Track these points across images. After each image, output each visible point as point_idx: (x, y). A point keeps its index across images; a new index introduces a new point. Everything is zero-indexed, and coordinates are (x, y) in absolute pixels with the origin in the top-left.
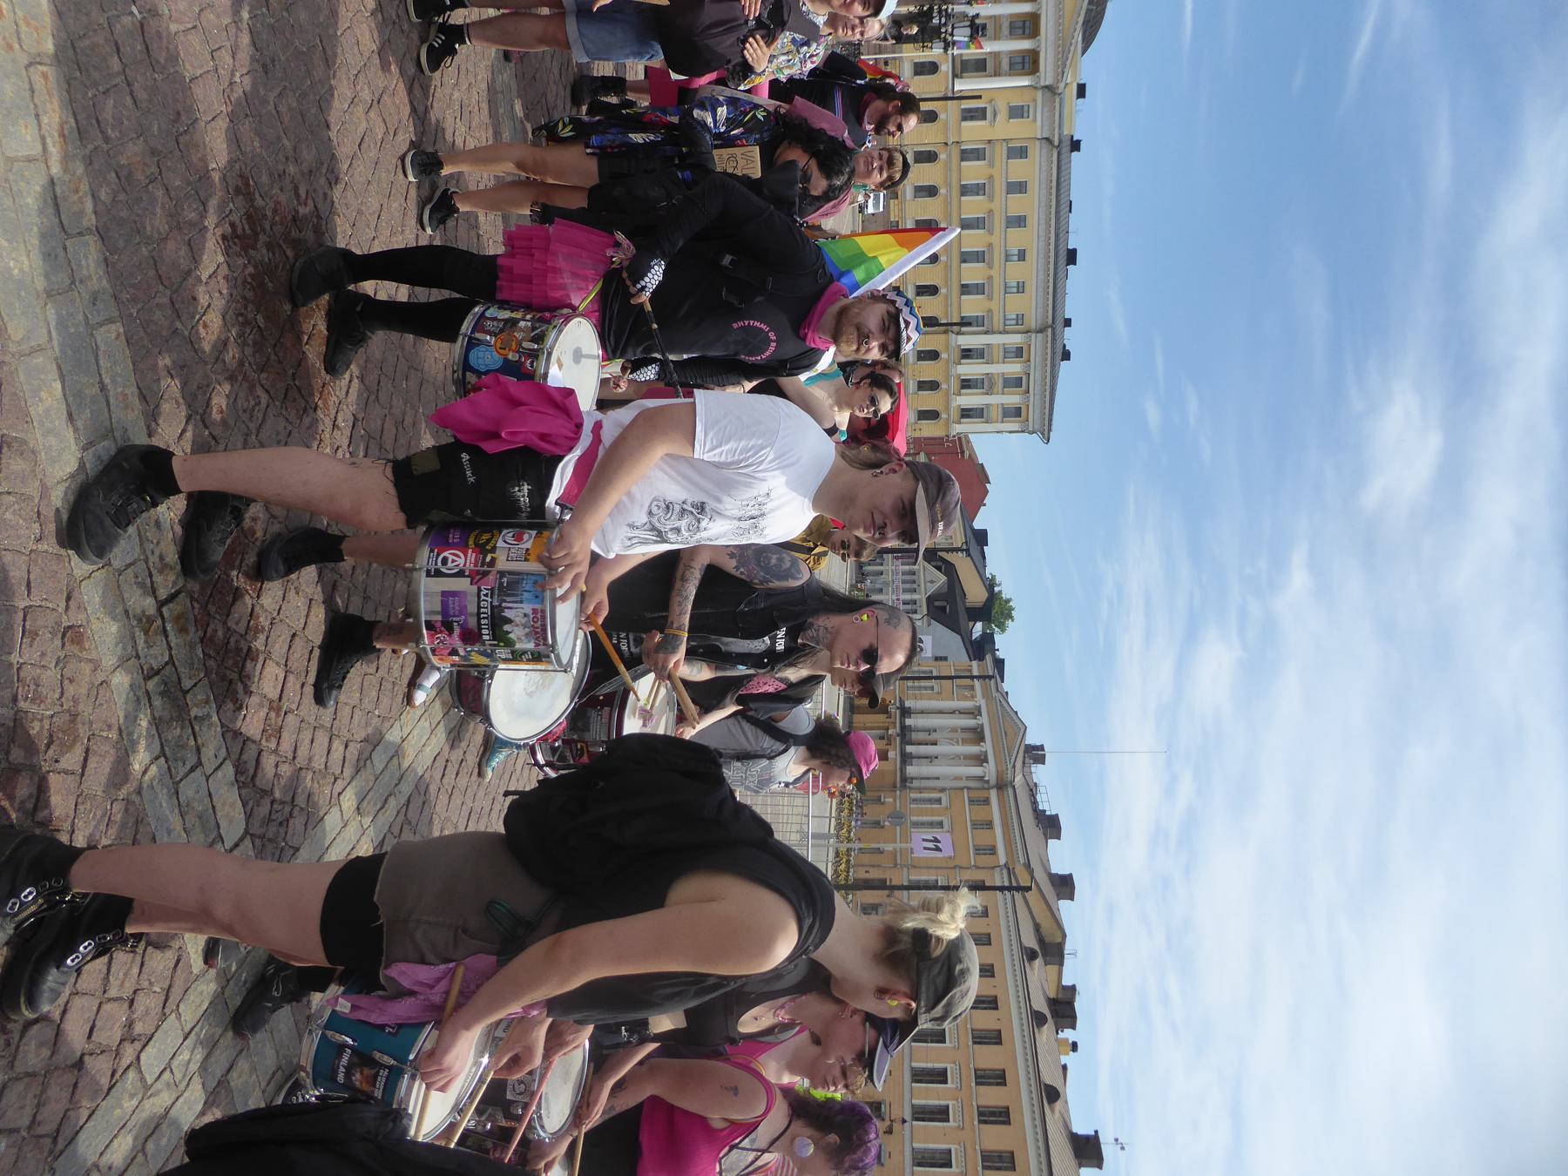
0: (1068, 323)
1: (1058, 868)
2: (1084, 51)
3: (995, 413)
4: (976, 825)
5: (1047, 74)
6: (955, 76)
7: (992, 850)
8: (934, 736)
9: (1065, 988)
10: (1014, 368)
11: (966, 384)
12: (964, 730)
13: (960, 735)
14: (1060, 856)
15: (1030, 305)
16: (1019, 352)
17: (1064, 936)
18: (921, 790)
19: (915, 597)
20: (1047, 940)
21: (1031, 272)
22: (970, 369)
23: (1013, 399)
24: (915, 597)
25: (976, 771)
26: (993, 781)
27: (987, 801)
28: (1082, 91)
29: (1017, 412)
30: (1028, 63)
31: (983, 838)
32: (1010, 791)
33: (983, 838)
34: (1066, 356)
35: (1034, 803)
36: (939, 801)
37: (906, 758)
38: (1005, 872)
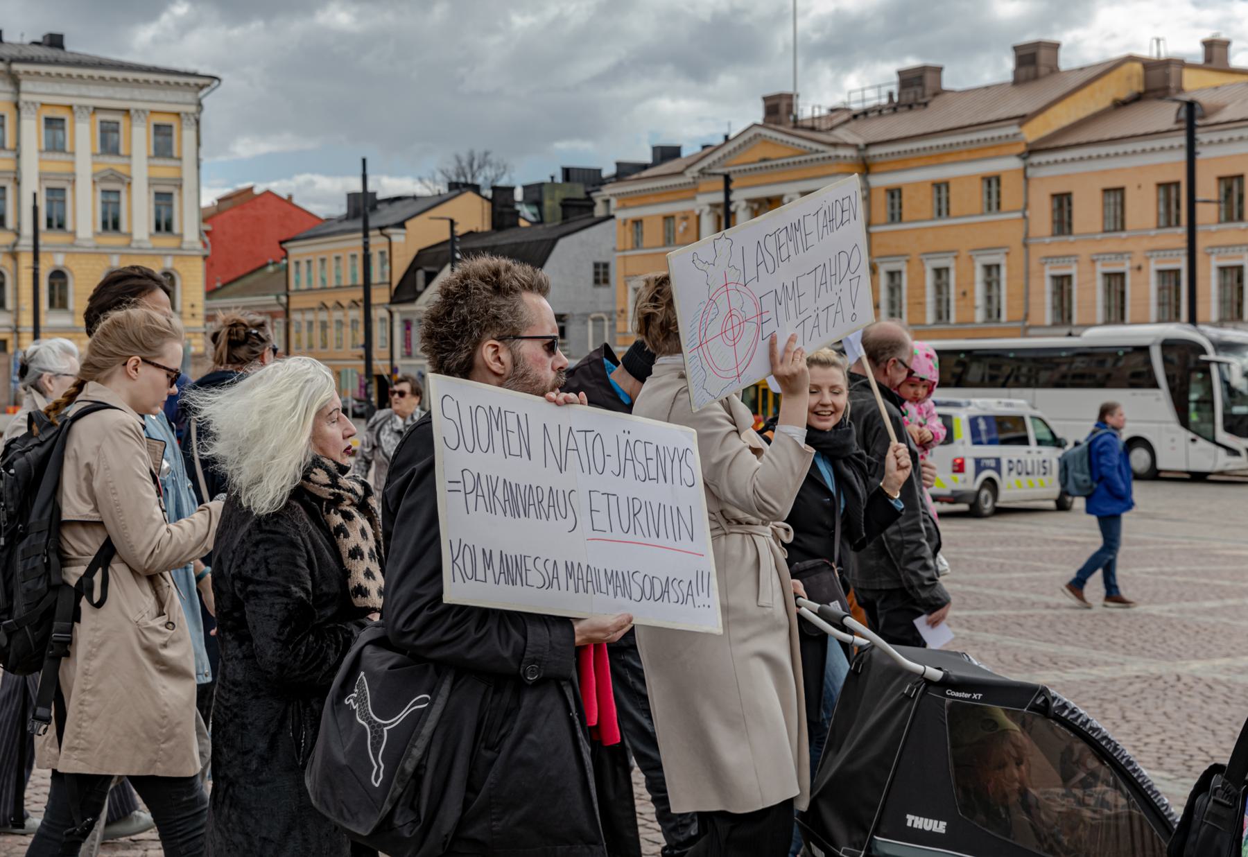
3: (165, 169)
4: (942, 208)
7: (993, 182)
10: (83, 134)
11: (111, 223)
17: (1131, 59)
23: (139, 138)
27: (894, 193)
29: (163, 132)
31: (967, 198)
32: (873, 151)
33: (967, 198)
34: (55, 41)
35: (879, 111)
36: (892, 275)
38: (1035, 159)
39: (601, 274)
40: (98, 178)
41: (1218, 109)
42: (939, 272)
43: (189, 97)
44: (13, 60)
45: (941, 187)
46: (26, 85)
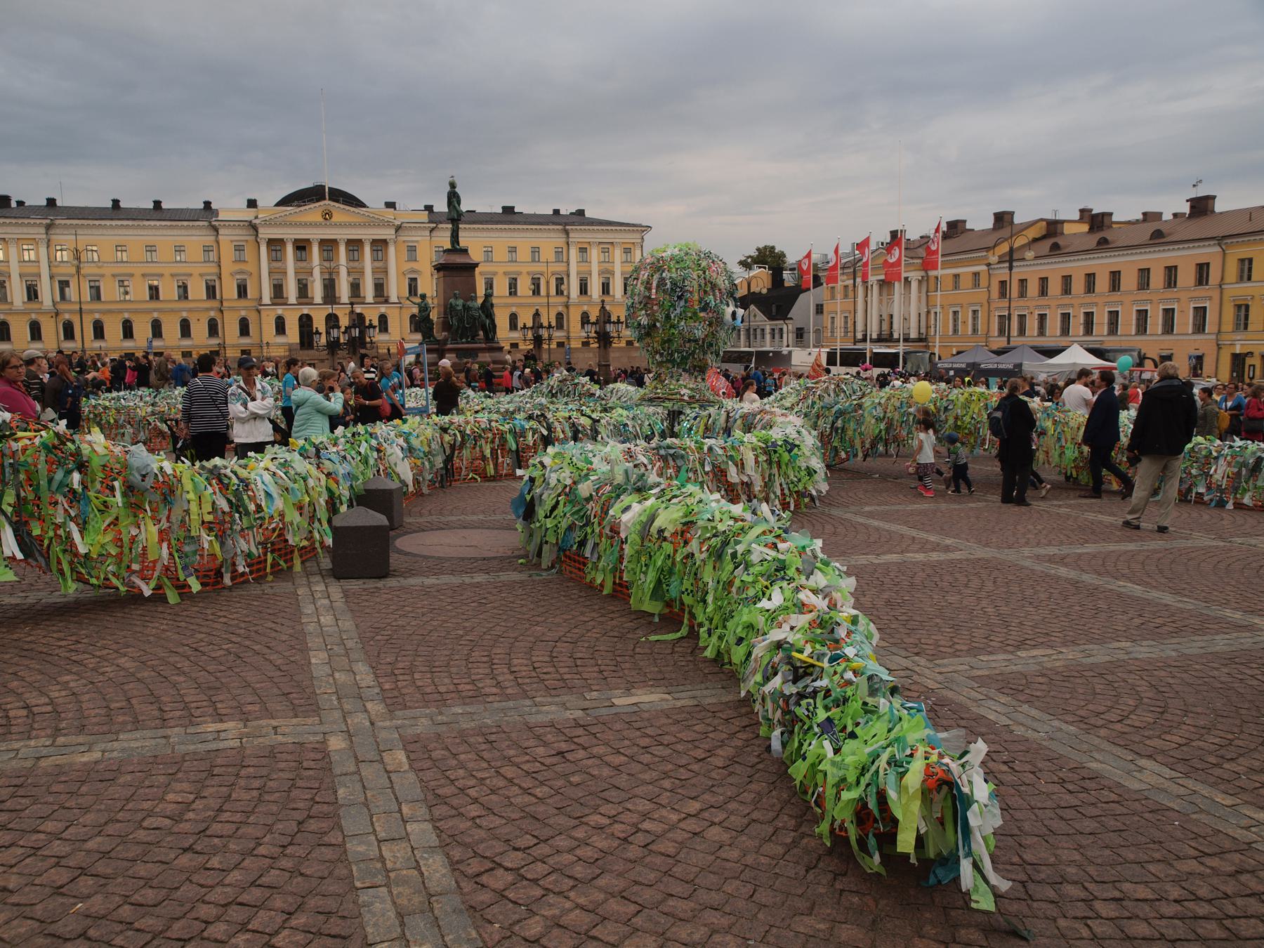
0: (556, 212)
1: (989, 224)
2: (362, 205)
4: (956, 287)
5: (387, 233)
6: (386, 301)
7: (976, 274)
8: (885, 317)
9: (1081, 218)
10: (594, 254)
12: (880, 294)
13: (885, 297)
14: (980, 221)
15: (549, 241)
16: (583, 250)
17: (1042, 220)
18: (928, 327)
19: (768, 330)
20: (1044, 233)
21: (524, 240)
24: (768, 330)
25: (914, 285)
26: (923, 273)
28: (390, 205)
30: (380, 245)
31: (966, 282)
33: (966, 282)
39: (819, 309)
40: (601, 273)
41: (1067, 247)
42: (955, 313)
43: (638, 236)
44: (566, 224)
45: (956, 276)
46: (571, 235)
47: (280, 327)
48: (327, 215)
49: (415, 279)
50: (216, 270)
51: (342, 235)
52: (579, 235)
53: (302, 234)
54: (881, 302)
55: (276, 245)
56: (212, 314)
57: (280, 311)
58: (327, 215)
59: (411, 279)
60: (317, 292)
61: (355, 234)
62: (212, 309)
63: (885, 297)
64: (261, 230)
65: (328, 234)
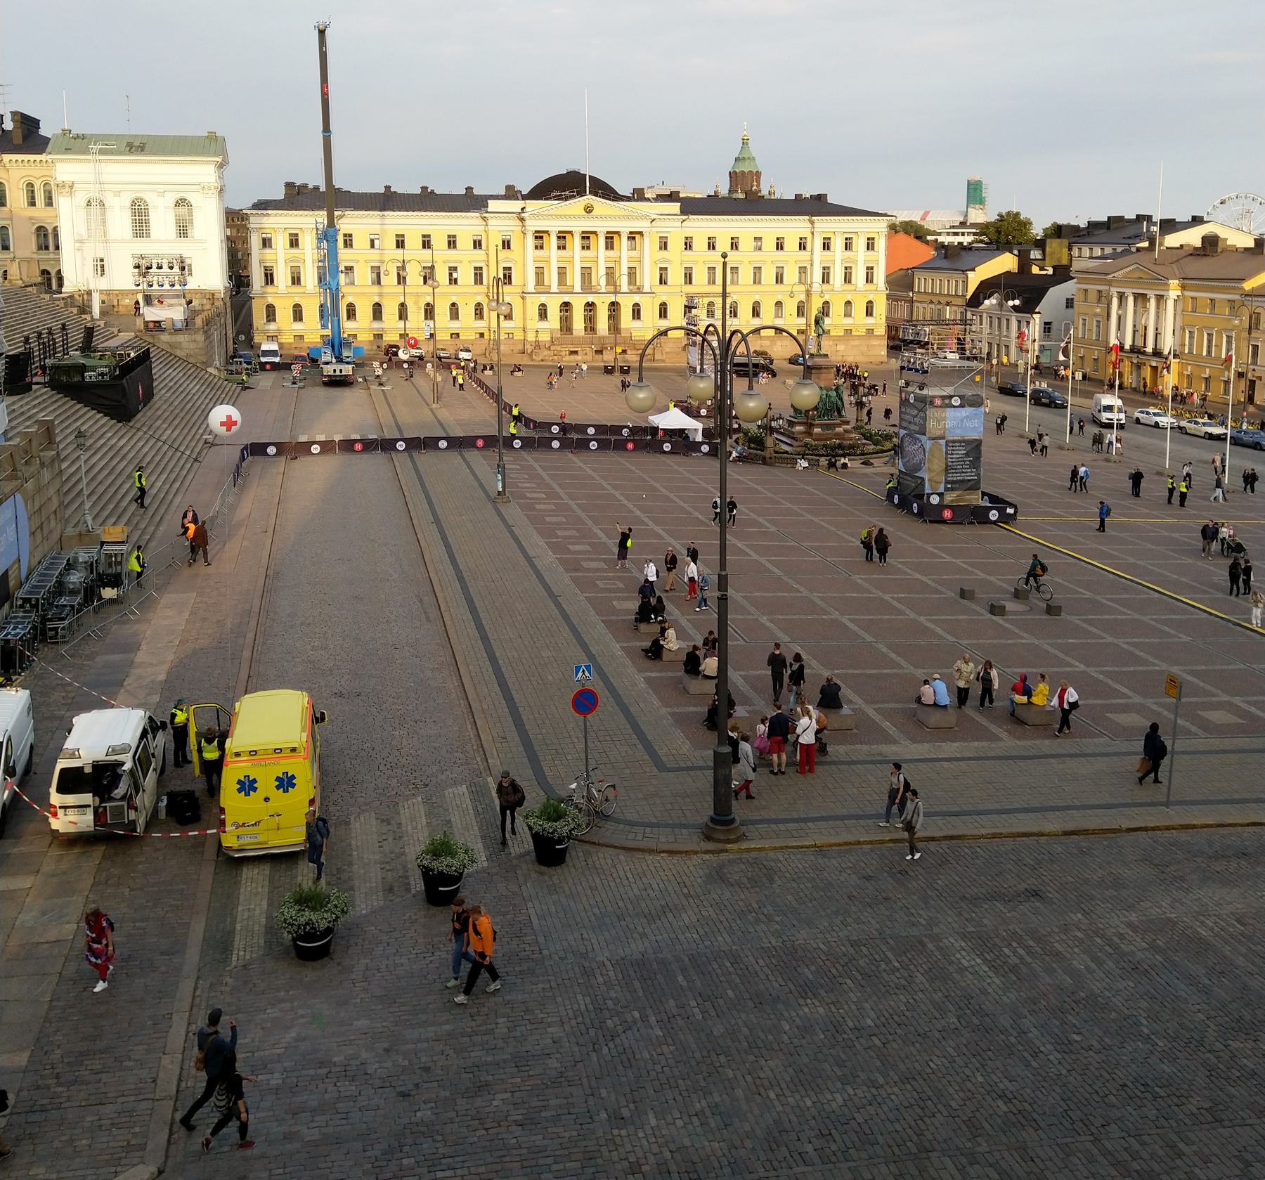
11: (848, 279)
22: (837, 276)
37: (1157, 353)
47: (543, 313)
48: (588, 209)
49: (666, 269)
50: (484, 258)
51: (602, 227)
52: (825, 225)
53: (564, 225)
54: (1135, 312)
55: (539, 235)
56: (479, 299)
57: (543, 299)
58: (588, 209)
59: (661, 269)
60: (576, 280)
61: (613, 226)
62: (479, 294)
63: (1140, 310)
64: (528, 223)
65: (589, 225)
